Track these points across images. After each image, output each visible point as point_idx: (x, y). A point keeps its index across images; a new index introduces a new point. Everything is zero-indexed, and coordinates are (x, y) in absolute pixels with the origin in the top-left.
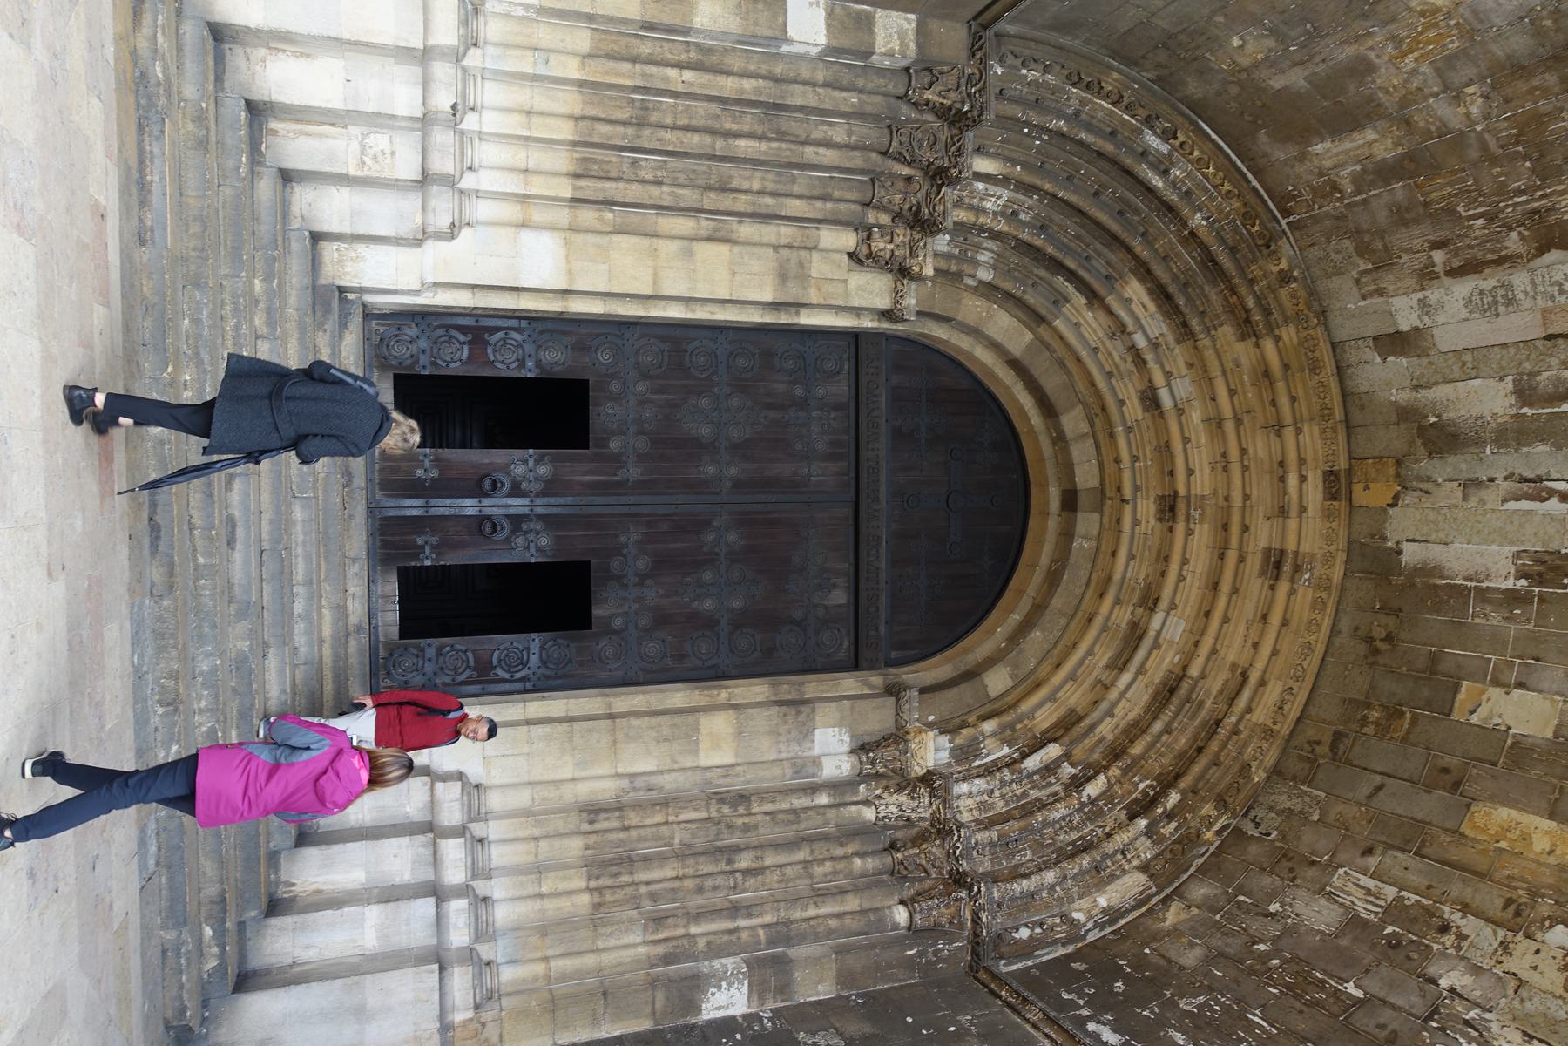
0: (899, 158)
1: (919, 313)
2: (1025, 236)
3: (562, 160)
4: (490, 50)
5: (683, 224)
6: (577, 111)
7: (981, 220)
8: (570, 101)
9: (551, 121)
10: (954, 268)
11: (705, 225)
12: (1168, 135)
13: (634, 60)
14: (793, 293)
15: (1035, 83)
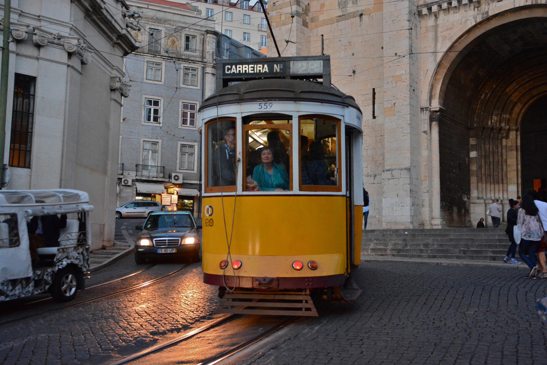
0: (490, 136)
1: (516, 126)
2: (500, 112)
3: (497, 186)
4: (483, 196)
5: (504, 167)
6: (489, 184)
7: (498, 120)
8: (488, 185)
9: (491, 187)
10: (507, 122)
11: (504, 164)
12: (481, 95)
13: (482, 177)
14: (514, 148)
15: (476, 118)
